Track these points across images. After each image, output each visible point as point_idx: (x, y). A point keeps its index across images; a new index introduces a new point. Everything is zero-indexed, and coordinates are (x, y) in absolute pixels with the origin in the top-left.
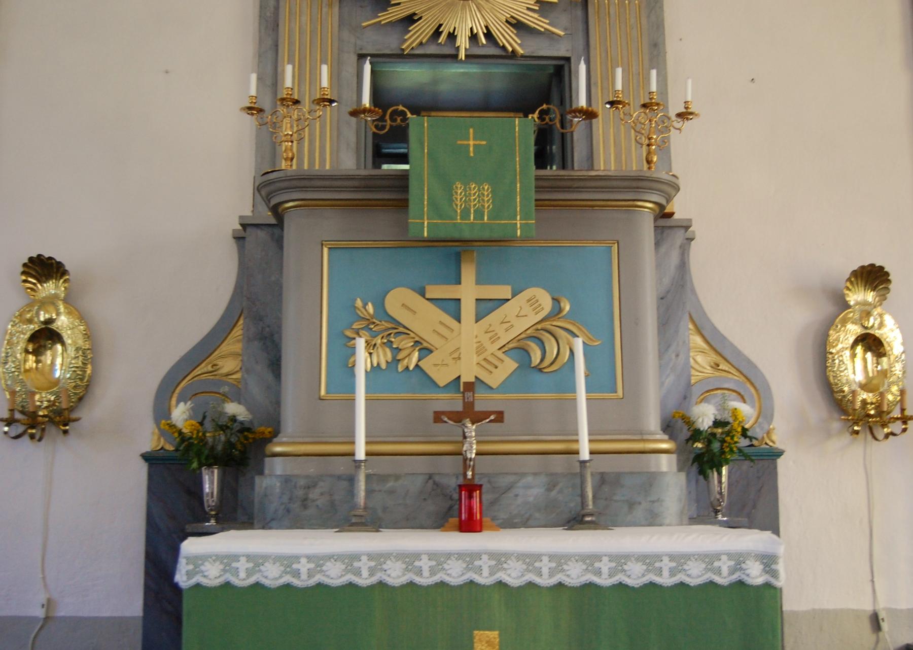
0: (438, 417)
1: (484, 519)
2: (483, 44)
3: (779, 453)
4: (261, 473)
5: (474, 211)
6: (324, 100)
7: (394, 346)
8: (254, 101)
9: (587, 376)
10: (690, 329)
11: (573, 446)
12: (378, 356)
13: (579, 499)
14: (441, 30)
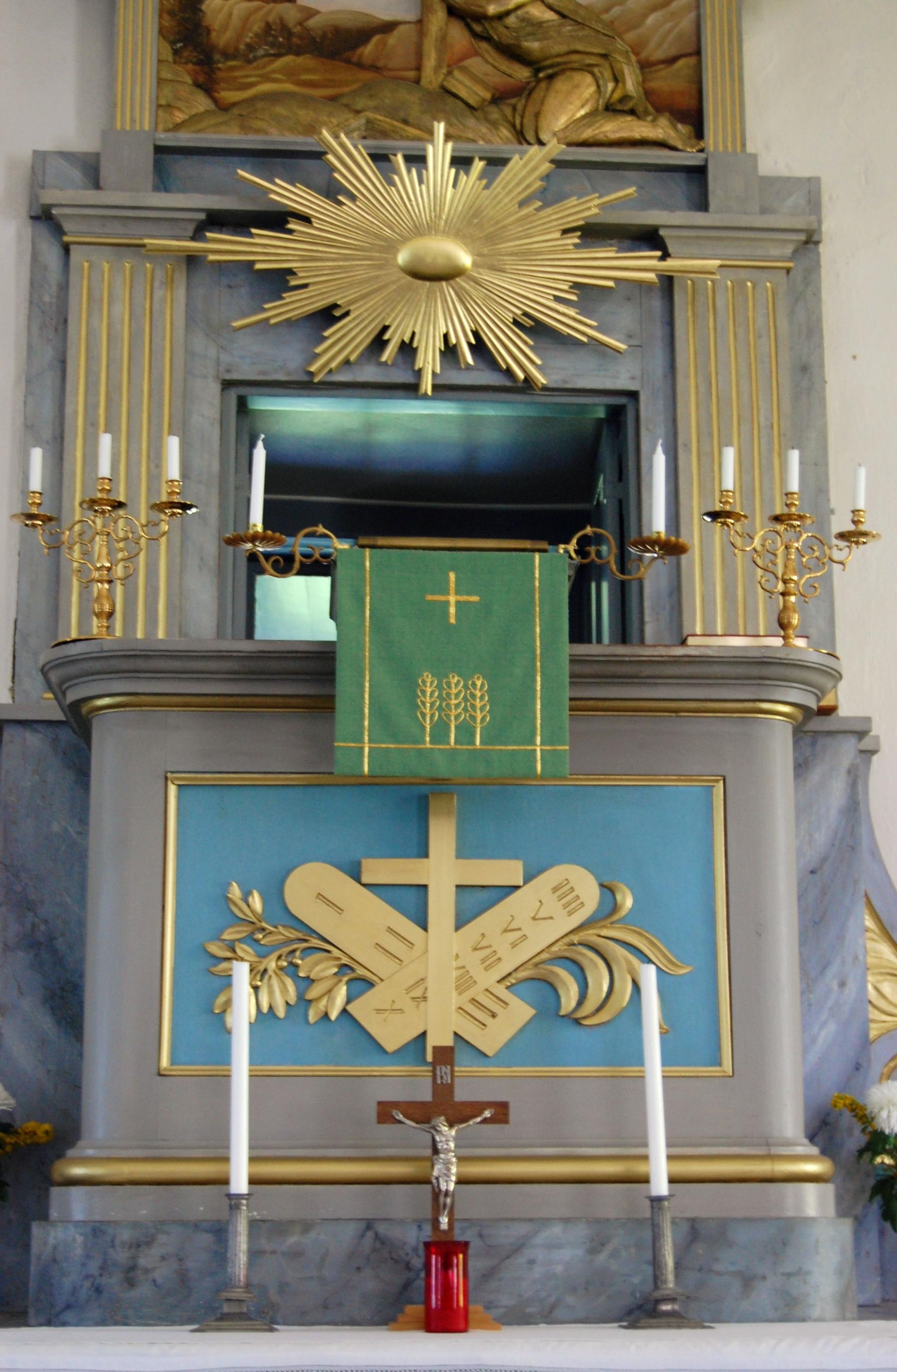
1: (471, 1307)
2: (468, 364)
4: (44, 1216)
5: (456, 727)
6: (172, 505)
7: (302, 974)
8: (38, 501)
9: (664, 1033)
10: (867, 930)
11: (639, 1168)
12: (271, 993)
13: (649, 1270)
14: (386, 337)
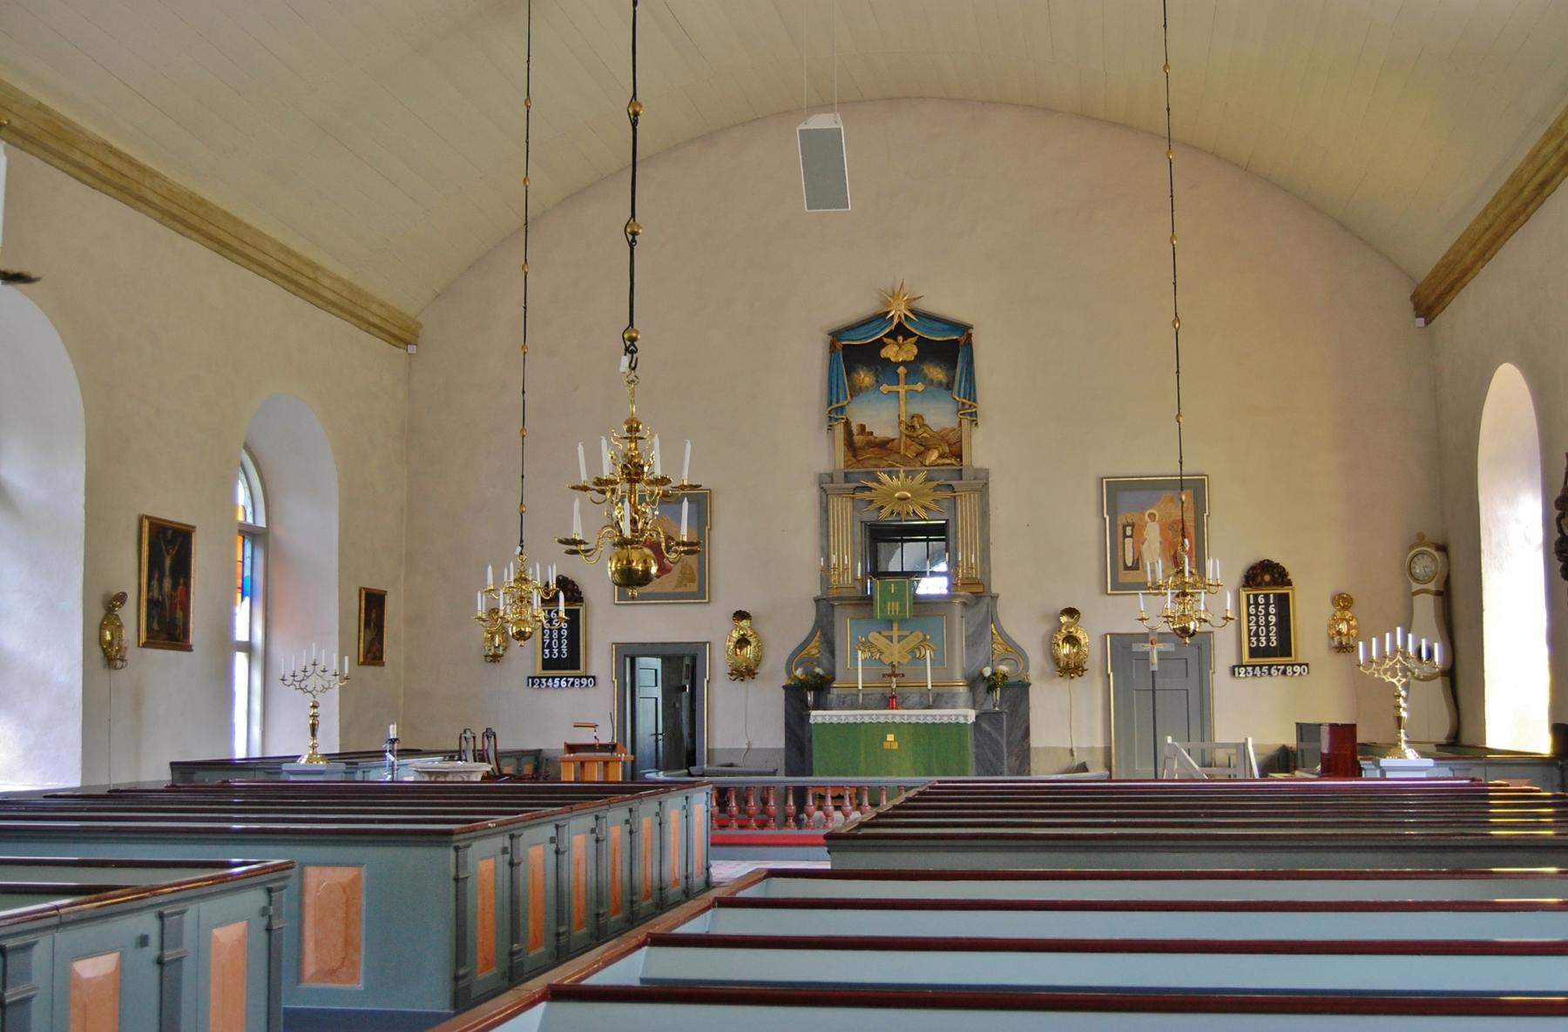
0: (884, 676)
3: (1030, 684)
4: (829, 693)
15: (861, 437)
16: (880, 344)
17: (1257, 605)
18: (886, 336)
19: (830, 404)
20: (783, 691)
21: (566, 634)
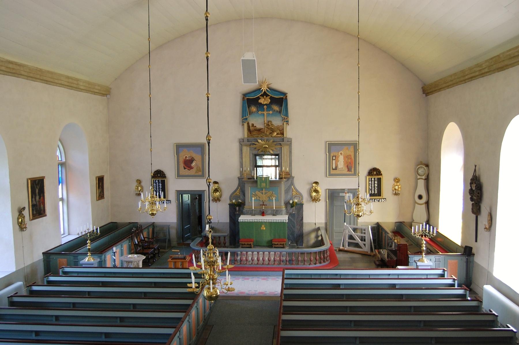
0: (260, 205)
15: (252, 128)
16: (258, 98)
17: (372, 181)
18: (260, 96)
19: (243, 117)
20: (229, 205)
21: (161, 187)
